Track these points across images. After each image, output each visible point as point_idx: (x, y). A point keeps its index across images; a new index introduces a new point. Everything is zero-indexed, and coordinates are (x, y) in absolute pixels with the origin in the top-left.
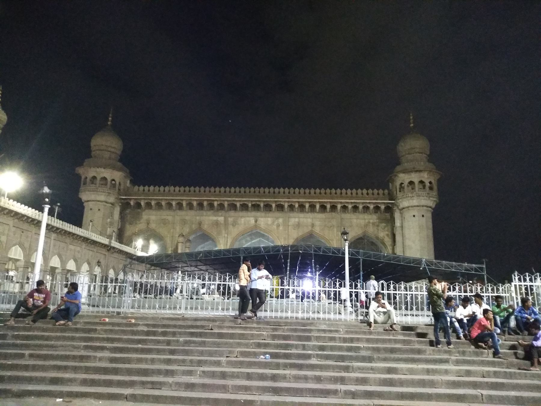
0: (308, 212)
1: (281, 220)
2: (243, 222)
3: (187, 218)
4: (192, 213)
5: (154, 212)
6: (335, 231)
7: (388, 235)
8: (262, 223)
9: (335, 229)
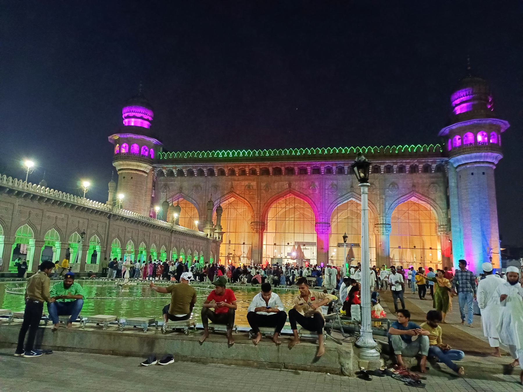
0: (347, 174)
2: (276, 187)
3: (220, 184)
7: (440, 197)
8: (297, 187)
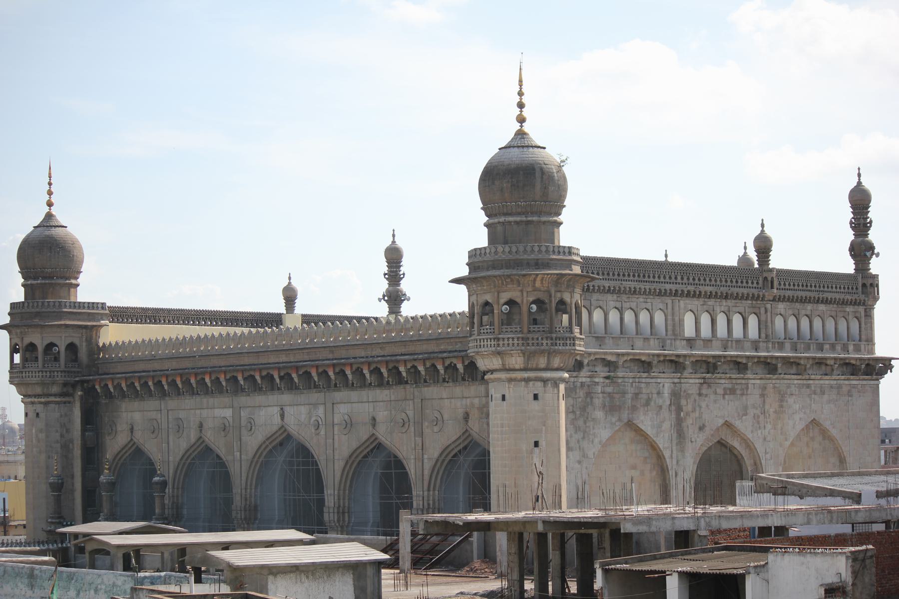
1: (321, 411)
4: (188, 402)
5: (136, 404)
6: (413, 434)
9: (412, 429)
